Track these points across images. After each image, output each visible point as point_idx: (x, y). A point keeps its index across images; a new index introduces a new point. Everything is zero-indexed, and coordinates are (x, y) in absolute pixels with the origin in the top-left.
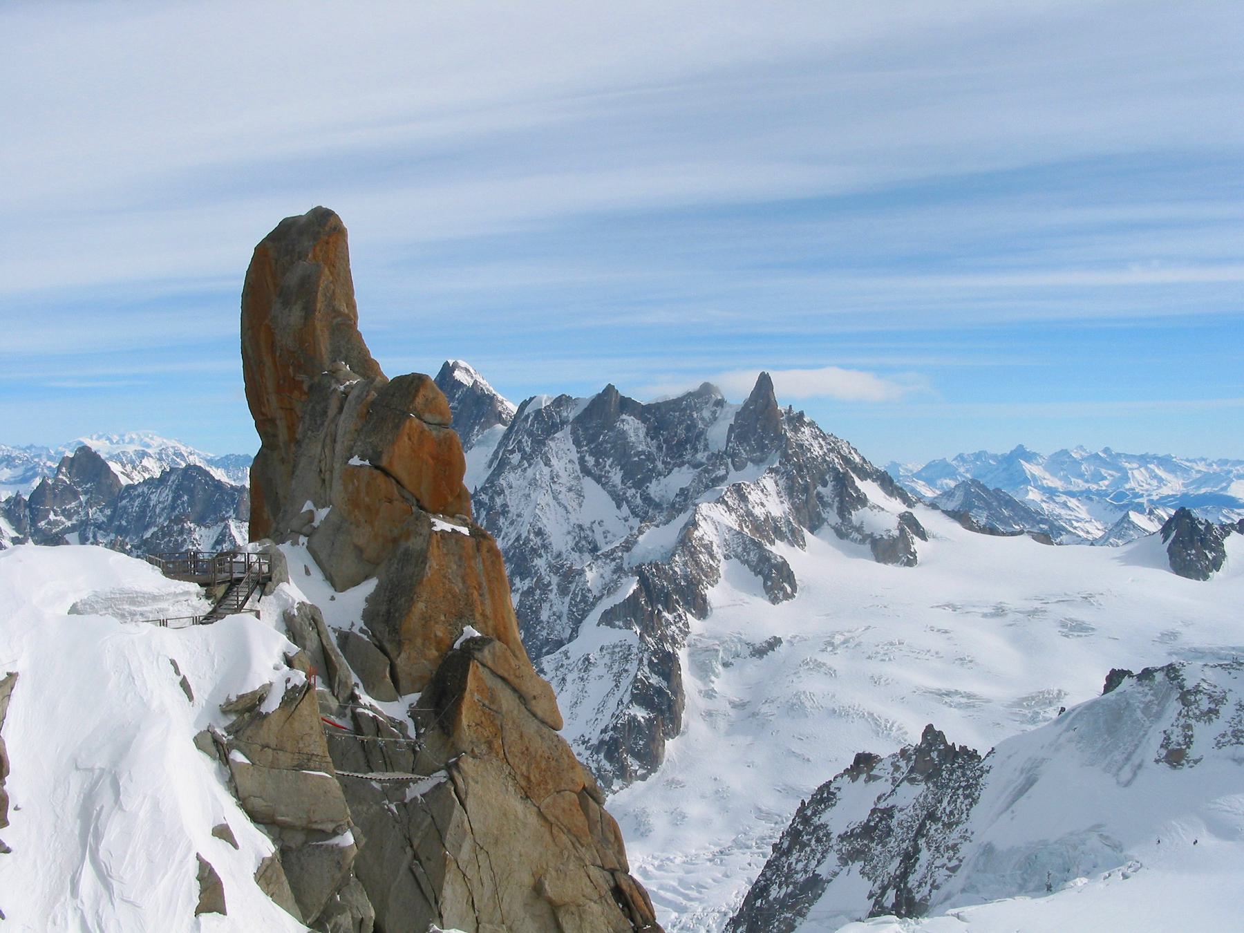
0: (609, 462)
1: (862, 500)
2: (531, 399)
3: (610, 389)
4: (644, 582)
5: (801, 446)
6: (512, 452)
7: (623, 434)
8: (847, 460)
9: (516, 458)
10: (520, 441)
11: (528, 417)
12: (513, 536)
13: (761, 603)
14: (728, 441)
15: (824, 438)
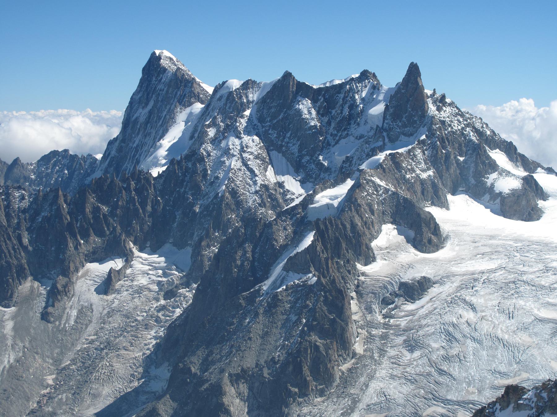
0: (288, 135)
1: (493, 166)
2: (224, 83)
3: (288, 76)
4: (321, 235)
5: (443, 122)
6: (209, 126)
7: (299, 113)
8: (480, 133)
9: (212, 132)
10: (215, 118)
11: (221, 97)
12: (212, 195)
13: (411, 254)
14: (384, 118)
15: (462, 115)
